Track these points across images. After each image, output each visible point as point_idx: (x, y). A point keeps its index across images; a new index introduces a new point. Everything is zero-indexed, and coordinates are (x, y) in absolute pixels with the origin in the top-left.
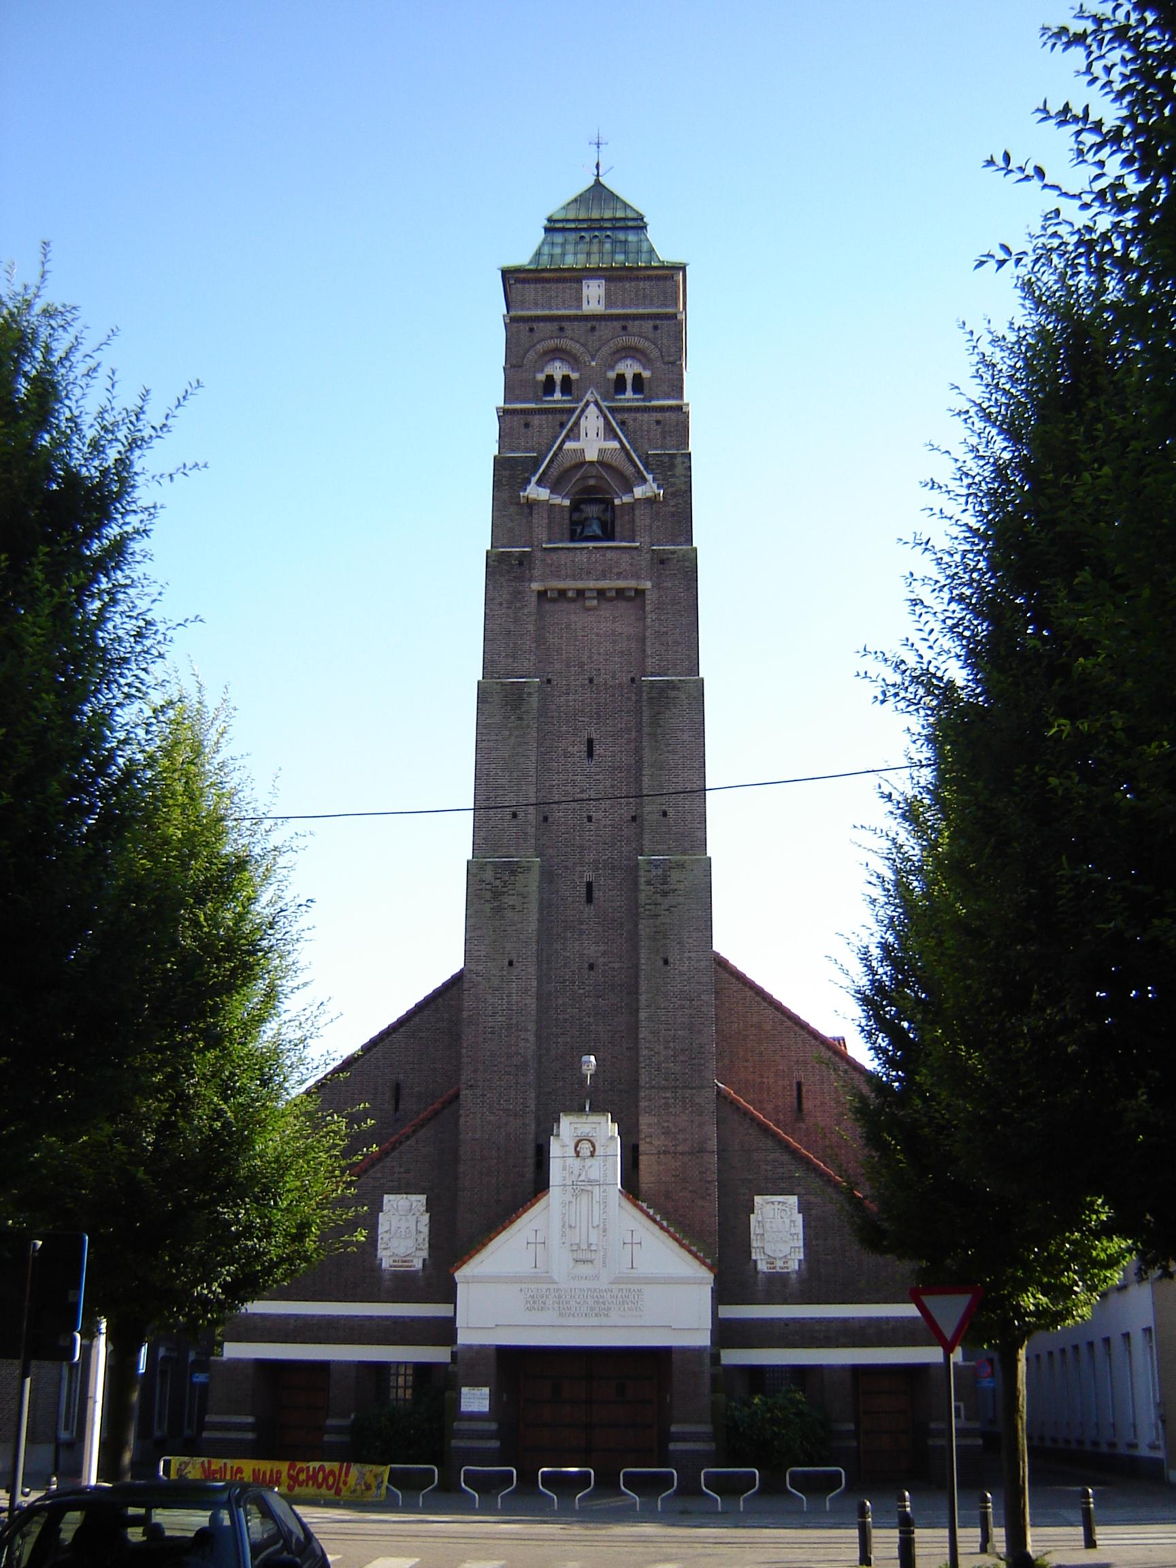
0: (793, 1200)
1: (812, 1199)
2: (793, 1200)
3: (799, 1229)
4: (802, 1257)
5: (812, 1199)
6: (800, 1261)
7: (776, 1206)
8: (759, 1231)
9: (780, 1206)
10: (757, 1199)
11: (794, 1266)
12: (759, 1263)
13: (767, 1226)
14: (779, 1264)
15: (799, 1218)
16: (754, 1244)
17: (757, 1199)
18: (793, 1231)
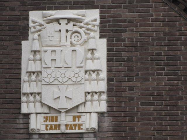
0: (93, 15)
1: (125, 14)
2: (93, 15)
3: (101, 62)
4: (103, 107)
5: (125, 14)
6: (101, 115)
7: (64, 26)
8: (33, 67)
9: (70, 27)
10: (35, 17)
11: (90, 122)
12: (33, 117)
13: (47, 57)
14: (65, 119)
15: (101, 45)
16: (26, 88)
17: (35, 17)
18: (90, 65)
